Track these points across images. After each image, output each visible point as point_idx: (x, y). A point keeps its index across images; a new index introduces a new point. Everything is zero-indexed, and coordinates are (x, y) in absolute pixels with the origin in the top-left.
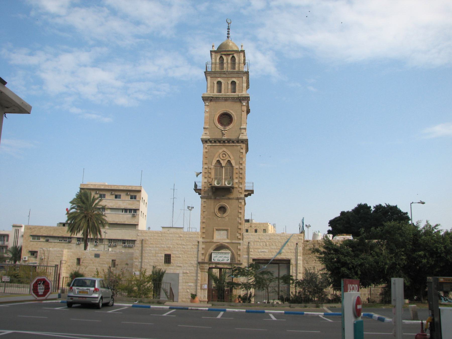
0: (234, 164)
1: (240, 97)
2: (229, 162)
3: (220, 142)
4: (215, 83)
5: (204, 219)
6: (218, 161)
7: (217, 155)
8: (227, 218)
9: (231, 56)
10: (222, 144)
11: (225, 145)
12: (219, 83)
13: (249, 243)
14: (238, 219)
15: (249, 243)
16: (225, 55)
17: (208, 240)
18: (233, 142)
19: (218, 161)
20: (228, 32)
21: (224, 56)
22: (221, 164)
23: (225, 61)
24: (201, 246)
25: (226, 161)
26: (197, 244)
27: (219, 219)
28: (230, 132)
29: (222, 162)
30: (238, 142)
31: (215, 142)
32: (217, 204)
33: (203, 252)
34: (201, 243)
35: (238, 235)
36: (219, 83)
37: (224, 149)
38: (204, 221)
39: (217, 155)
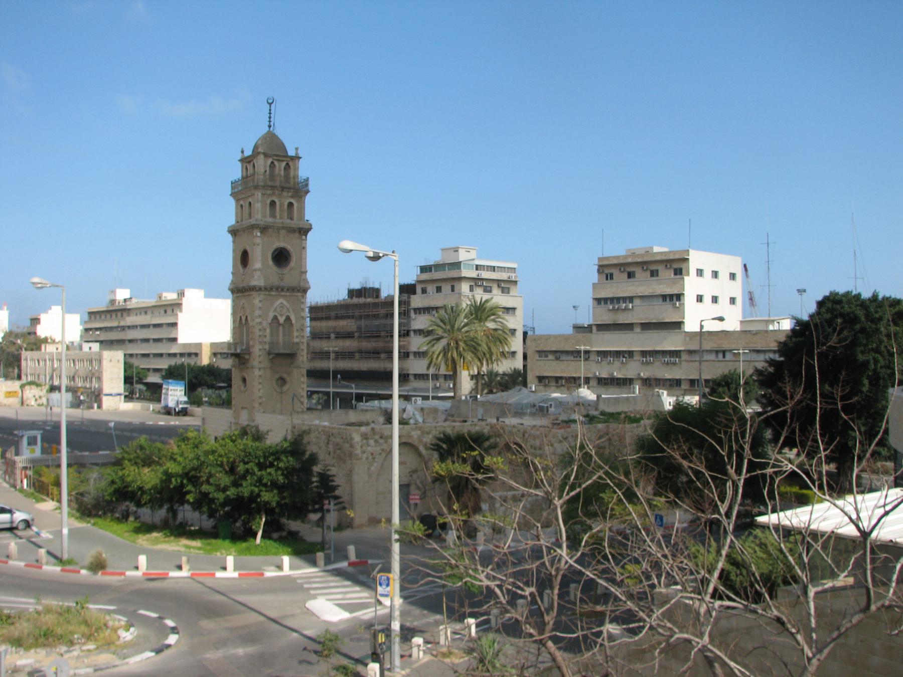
0: (294, 321)
4: (268, 202)
6: (275, 318)
9: (284, 164)
11: (283, 293)
12: (273, 203)
16: (278, 160)
19: (275, 318)
23: (277, 171)
25: (284, 318)
28: (288, 276)
29: (279, 318)
30: (298, 291)
31: (271, 289)
36: (273, 203)
37: (281, 300)
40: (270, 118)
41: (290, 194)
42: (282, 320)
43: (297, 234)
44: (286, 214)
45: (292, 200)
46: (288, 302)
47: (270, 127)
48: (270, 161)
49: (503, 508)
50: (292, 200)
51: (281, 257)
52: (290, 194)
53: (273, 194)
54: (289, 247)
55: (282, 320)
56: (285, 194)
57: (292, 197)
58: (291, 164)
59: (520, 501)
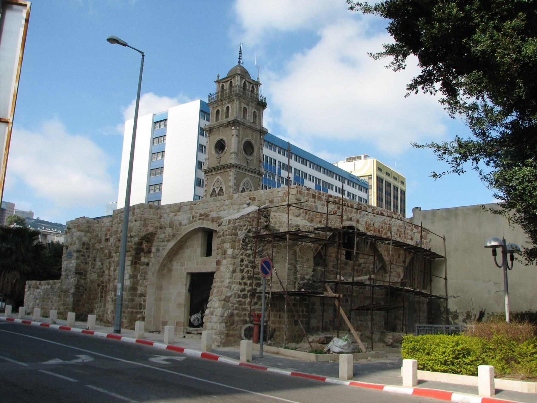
2: (221, 189)
6: (214, 190)
9: (229, 82)
11: (219, 172)
16: (225, 82)
19: (214, 190)
21: (224, 84)
25: (219, 189)
37: (218, 177)
40: (240, 56)
41: (227, 101)
42: (217, 191)
43: (230, 127)
44: (225, 116)
45: (228, 105)
46: (222, 178)
47: (239, 62)
48: (221, 84)
49: (28, 293)
50: (228, 105)
51: (220, 146)
52: (227, 101)
53: (218, 106)
54: (225, 138)
55: (217, 191)
56: (224, 102)
57: (229, 103)
58: (233, 81)
59: (38, 288)
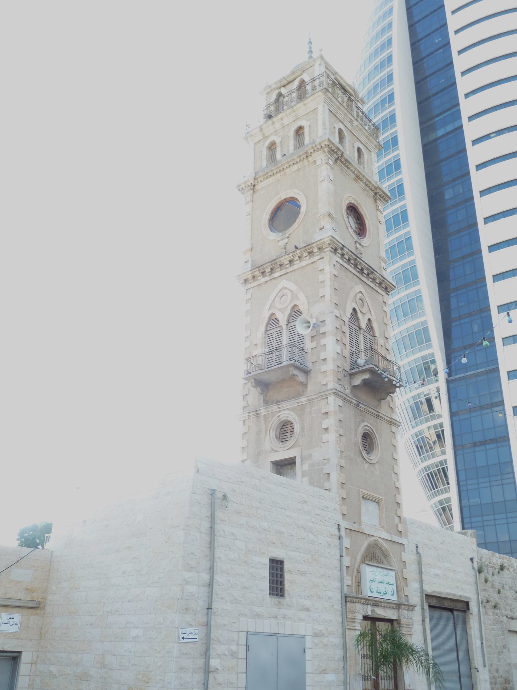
1: (380, 189)
3: (356, 266)
5: (341, 458)
7: (352, 295)
8: (377, 466)
10: (357, 274)
13: (417, 547)
14: (393, 475)
15: (417, 547)
17: (355, 527)
18: (374, 280)
20: (310, 48)
22: (357, 319)
24: (347, 542)
26: (336, 532)
27: (367, 465)
29: (360, 315)
32: (359, 423)
33: (347, 561)
34: (343, 533)
35: (397, 520)
37: (360, 287)
38: (343, 462)
39: (352, 295)
